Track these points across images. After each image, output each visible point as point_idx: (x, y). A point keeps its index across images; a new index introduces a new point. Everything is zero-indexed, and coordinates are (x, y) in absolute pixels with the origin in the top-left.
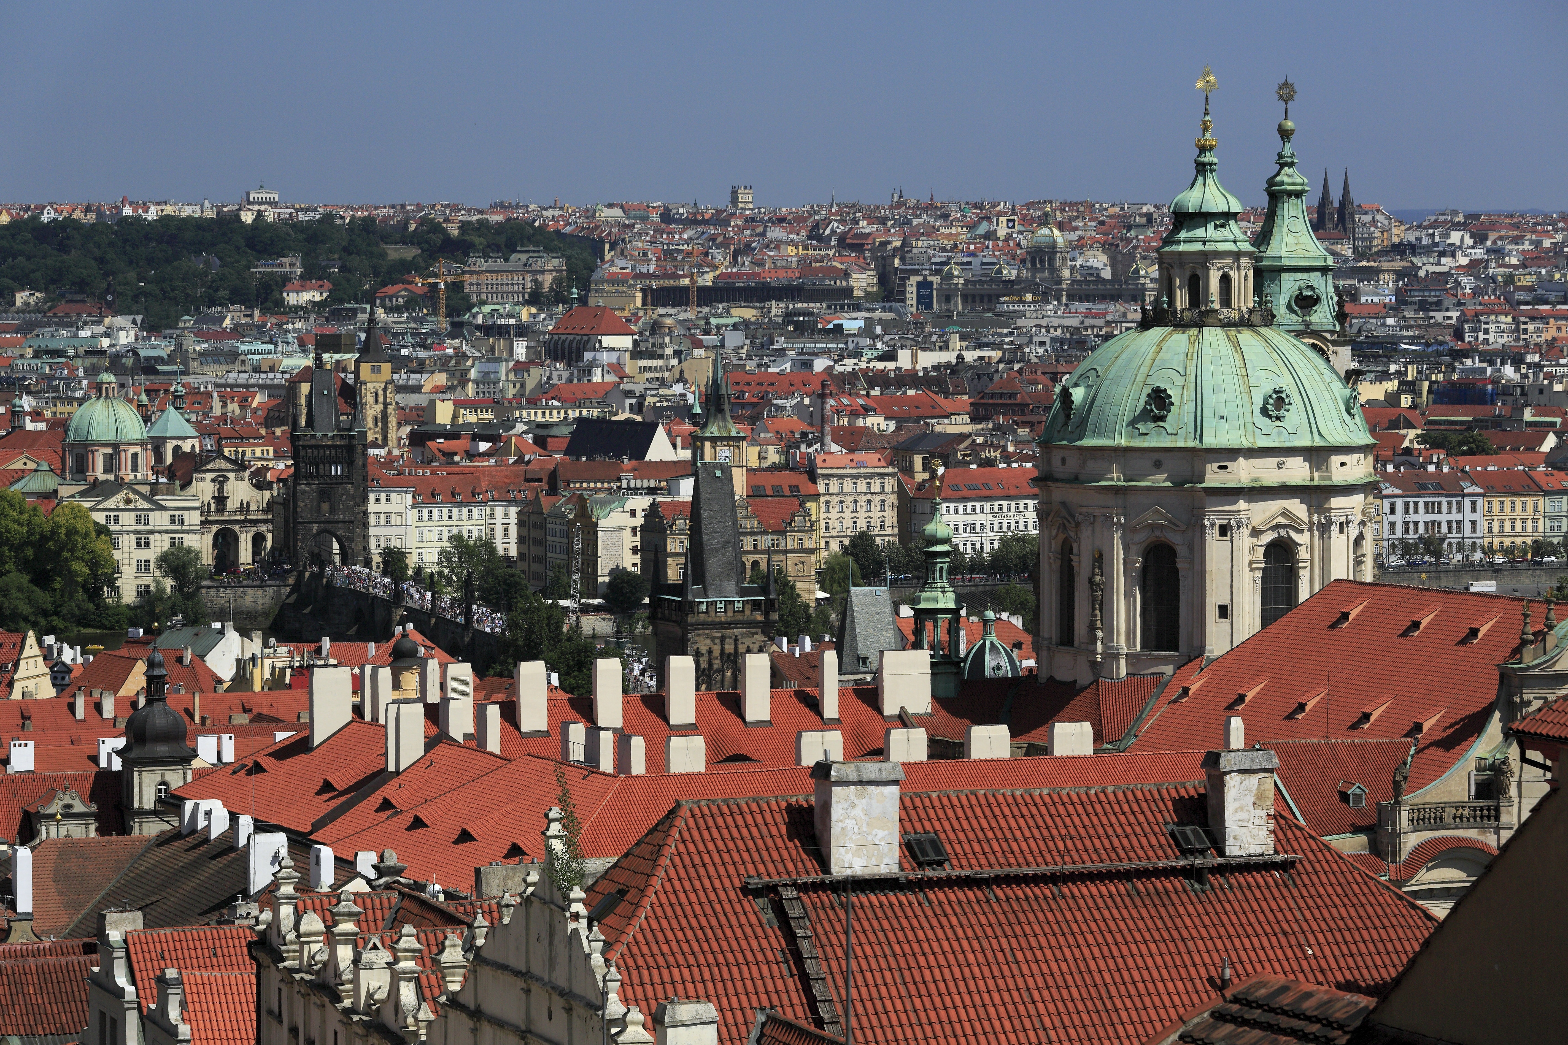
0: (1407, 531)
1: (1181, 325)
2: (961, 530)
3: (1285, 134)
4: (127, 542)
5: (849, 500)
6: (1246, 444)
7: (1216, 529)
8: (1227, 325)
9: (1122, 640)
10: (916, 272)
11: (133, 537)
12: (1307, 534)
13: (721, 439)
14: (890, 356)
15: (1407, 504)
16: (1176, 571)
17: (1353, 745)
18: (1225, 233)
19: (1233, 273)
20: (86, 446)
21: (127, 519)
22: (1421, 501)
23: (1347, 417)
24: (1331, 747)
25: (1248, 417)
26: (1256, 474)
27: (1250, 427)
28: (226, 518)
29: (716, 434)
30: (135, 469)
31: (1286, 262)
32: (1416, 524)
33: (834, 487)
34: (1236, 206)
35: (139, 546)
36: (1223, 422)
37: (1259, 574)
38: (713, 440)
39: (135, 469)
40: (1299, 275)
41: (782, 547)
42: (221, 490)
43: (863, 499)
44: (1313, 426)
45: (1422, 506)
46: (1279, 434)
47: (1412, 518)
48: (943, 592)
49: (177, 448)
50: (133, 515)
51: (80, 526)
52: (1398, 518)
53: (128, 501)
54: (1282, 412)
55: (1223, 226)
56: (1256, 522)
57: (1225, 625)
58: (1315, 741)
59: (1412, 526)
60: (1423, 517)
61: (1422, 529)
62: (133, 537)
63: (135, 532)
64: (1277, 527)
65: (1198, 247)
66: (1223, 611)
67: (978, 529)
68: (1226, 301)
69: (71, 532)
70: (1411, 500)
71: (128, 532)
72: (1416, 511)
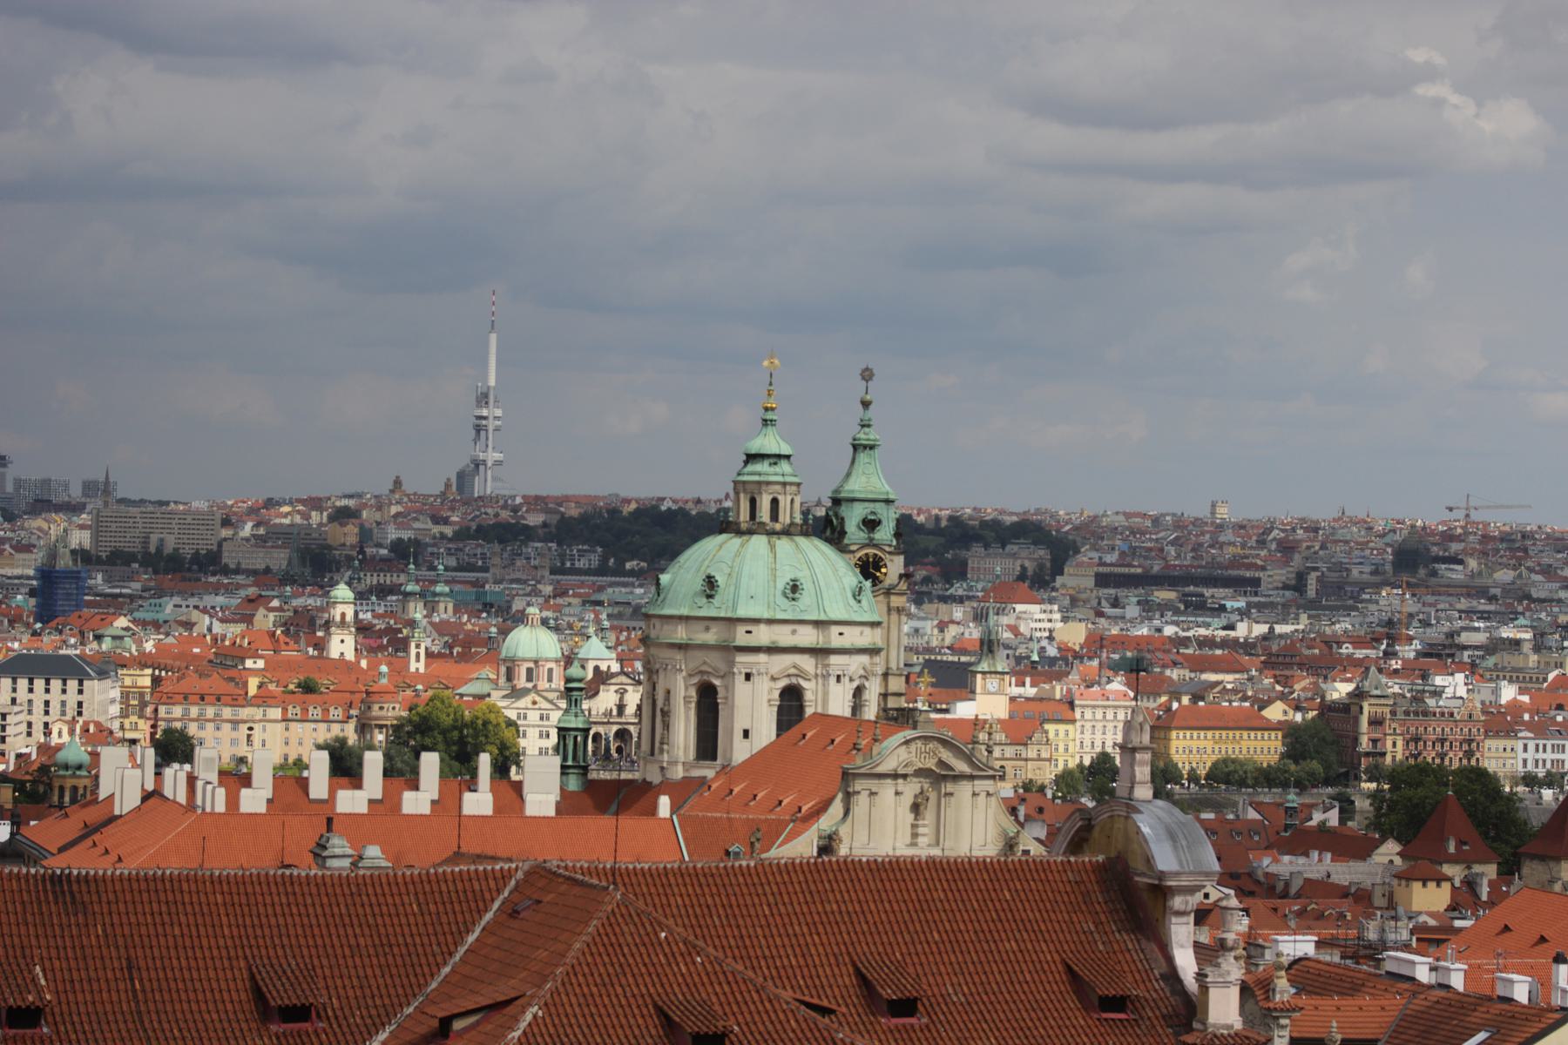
0: (1537, 767)
1: (739, 532)
2: (1181, 751)
3: (866, 404)
4: (533, 733)
5: (1099, 726)
6: (766, 615)
7: (743, 676)
8: (771, 533)
9: (681, 753)
10: (1315, 569)
11: (537, 730)
12: (814, 681)
13: (991, 673)
14: (1231, 627)
15: (1537, 746)
16: (717, 704)
17: (748, 819)
18: (777, 469)
19: (780, 498)
20: (514, 661)
21: (533, 716)
22: (1549, 744)
23: (852, 602)
24: (729, 819)
25: (772, 598)
26: (775, 638)
27: (772, 604)
28: (623, 720)
29: (986, 669)
30: (550, 680)
31: (858, 495)
32: (1544, 761)
33: (1088, 714)
34: (786, 450)
35: (541, 736)
36: (752, 601)
37: (776, 709)
38: (984, 673)
39: (550, 680)
40: (866, 504)
41: (1024, 756)
42: (621, 699)
43: (1099, 726)
44: (820, 606)
45: (1549, 748)
46: (794, 610)
47: (1540, 756)
48: (576, 716)
49: (596, 668)
50: (538, 713)
51: (492, 717)
52: (1530, 755)
53: (534, 703)
54: (797, 595)
55: (775, 464)
56: (774, 671)
57: (746, 743)
58: (719, 815)
59: (1540, 763)
60: (1549, 756)
61: (1548, 765)
62: (537, 730)
63: (539, 726)
64: (789, 676)
65: (756, 478)
66: (746, 734)
67: (1194, 751)
68: (775, 516)
69: (486, 723)
70: (1541, 742)
71: (534, 726)
72: (1545, 751)
